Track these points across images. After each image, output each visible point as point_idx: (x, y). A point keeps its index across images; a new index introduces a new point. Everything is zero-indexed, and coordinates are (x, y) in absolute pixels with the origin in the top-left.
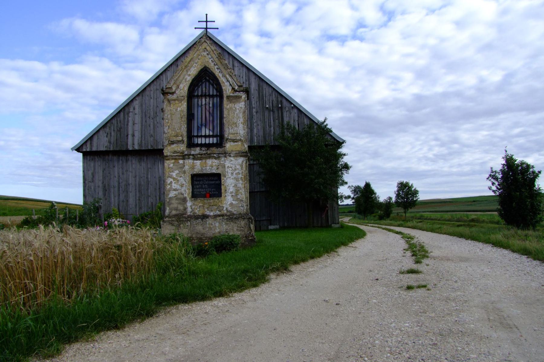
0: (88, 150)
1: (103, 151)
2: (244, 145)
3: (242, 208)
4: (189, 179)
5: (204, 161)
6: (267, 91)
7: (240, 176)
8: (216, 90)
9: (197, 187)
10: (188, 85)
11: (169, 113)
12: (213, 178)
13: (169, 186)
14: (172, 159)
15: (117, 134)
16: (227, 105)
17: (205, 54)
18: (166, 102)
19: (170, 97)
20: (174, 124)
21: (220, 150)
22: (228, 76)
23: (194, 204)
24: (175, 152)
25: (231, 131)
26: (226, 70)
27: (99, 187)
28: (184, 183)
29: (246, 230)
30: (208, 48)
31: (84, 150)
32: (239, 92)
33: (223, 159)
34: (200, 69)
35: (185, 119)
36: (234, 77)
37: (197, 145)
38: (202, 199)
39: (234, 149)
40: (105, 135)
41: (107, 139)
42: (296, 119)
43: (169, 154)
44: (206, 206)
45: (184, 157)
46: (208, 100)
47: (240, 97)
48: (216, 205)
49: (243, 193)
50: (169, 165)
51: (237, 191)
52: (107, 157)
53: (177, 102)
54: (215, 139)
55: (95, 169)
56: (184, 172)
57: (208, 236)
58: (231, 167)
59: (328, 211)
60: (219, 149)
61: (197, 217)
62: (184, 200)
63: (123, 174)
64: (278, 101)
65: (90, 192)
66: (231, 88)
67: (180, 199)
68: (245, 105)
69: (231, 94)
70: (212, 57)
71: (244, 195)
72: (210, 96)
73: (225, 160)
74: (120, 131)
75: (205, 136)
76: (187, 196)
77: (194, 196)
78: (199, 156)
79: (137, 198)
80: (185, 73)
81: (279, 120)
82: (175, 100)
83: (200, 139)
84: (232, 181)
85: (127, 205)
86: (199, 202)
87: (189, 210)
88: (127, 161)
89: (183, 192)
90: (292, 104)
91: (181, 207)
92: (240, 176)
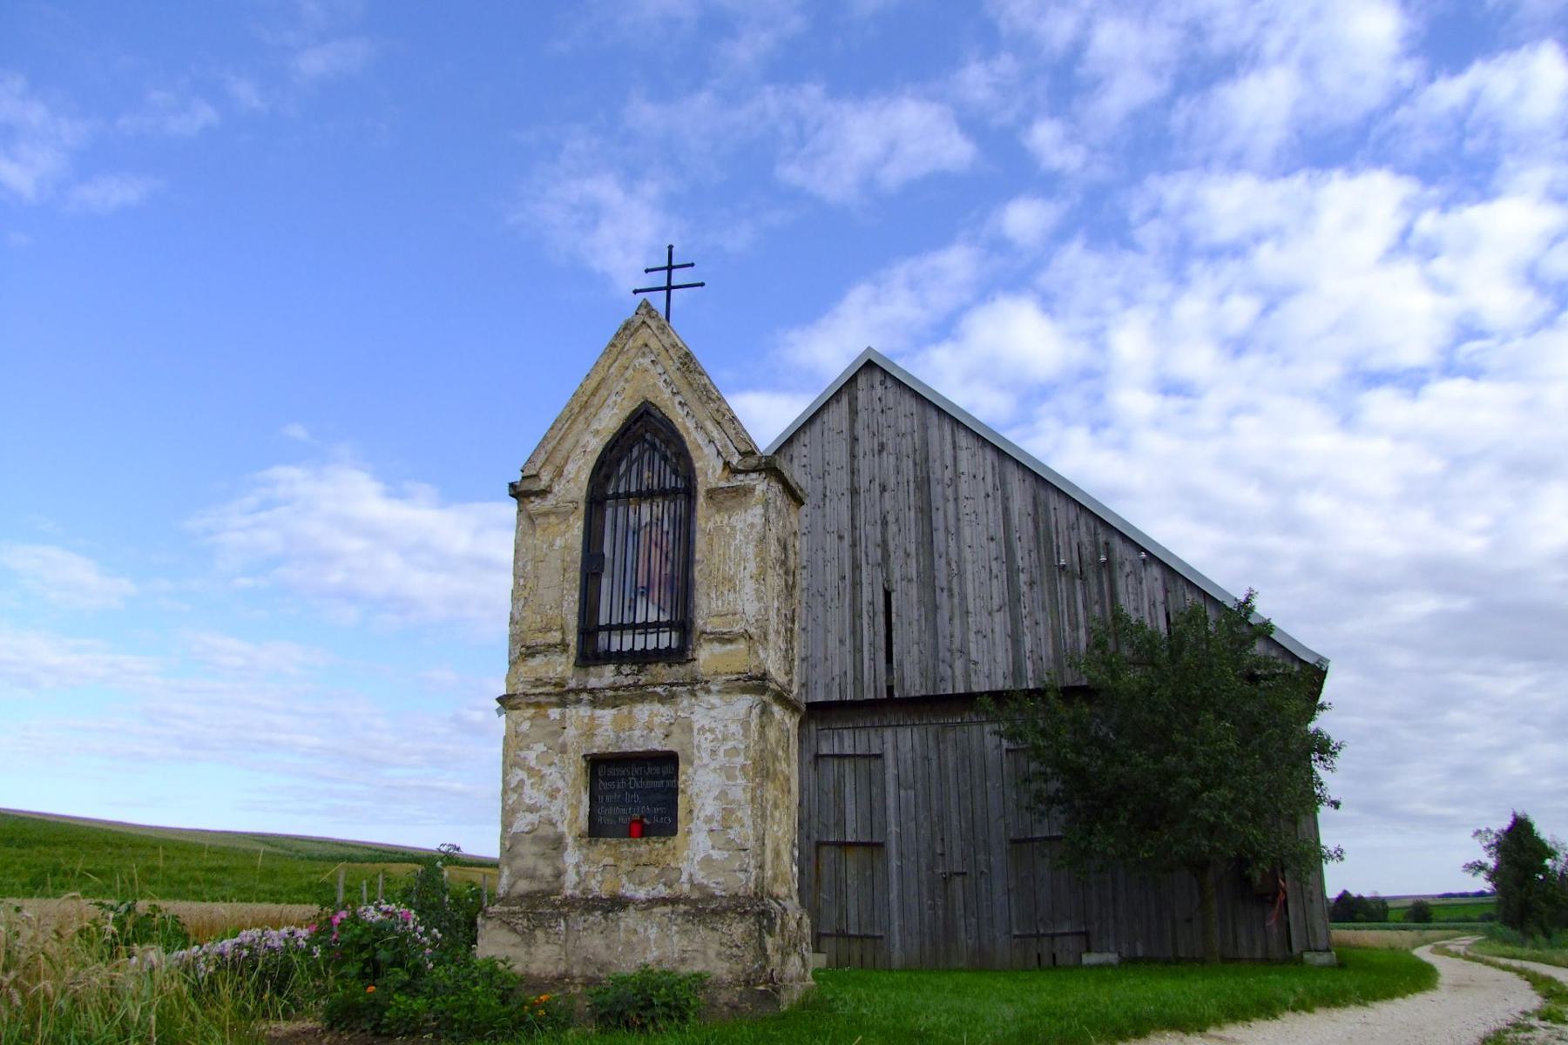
3: (742, 876)
4: (575, 768)
5: (625, 709)
6: (1061, 515)
8: (675, 472)
10: (592, 464)
13: (515, 797)
14: (529, 705)
17: (646, 362)
20: (540, 591)
21: (679, 671)
22: (709, 425)
24: (538, 682)
25: (717, 605)
26: (704, 404)
28: (560, 784)
29: (749, 957)
30: (654, 343)
32: (746, 472)
33: (685, 702)
34: (627, 413)
35: (575, 574)
36: (726, 425)
38: (614, 841)
39: (722, 669)
42: (1160, 597)
44: (625, 866)
45: (564, 696)
48: (655, 864)
49: (748, 822)
53: (553, 519)
56: (563, 750)
58: (712, 730)
59: (1285, 903)
60: (676, 668)
61: (590, 904)
62: (558, 844)
64: (1096, 544)
66: (719, 464)
69: (723, 484)
76: (566, 829)
77: (596, 830)
78: (610, 693)
80: (580, 424)
81: (1103, 607)
82: (546, 514)
84: (712, 776)
86: (603, 852)
87: (571, 878)
89: (556, 817)
91: (546, 870)
92: (740, 760)
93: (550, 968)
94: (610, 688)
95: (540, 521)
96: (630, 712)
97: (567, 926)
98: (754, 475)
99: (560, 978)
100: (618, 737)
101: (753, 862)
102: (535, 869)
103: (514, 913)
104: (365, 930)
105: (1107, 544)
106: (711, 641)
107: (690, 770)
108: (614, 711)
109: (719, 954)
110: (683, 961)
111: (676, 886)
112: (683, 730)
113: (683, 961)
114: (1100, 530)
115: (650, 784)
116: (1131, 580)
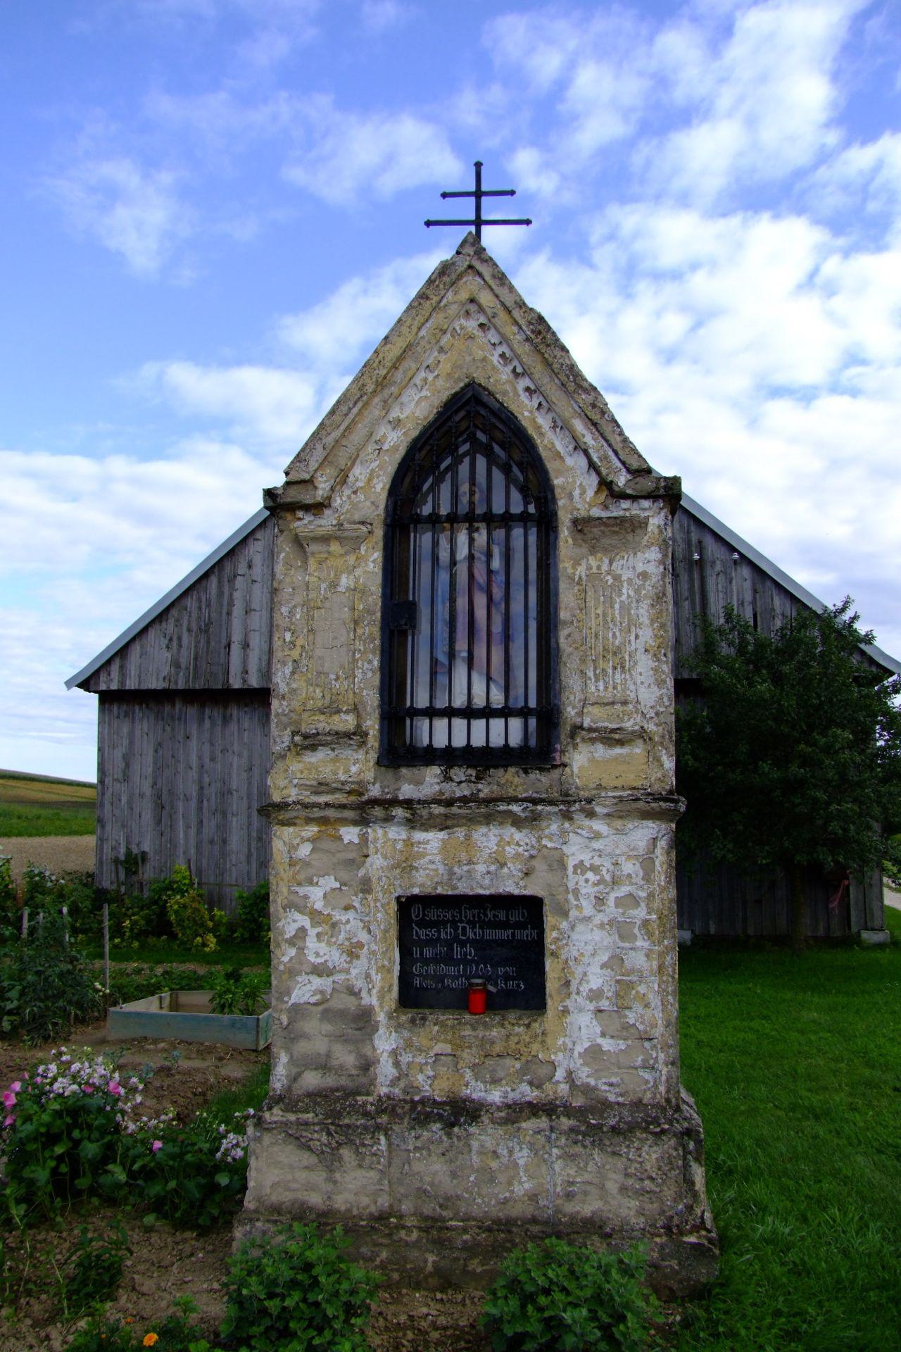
0: (114, 687)
1: (155, 691)
2: (658, 760)
3: (646, 1075)
4: (386, 917)
5: (460, 833)
7: (640, 913)
8: (524, 490)
9: (428, 952)
11: (298, 599)
12: (502, 915)
14: (309, 820)
15: (198, 643)
16: (577, 563)
17: (471, 325)
18: (285, 551)
19: (304, 524)
20: (318, 652)
21: (540, 781)
22: (579, 426)
23: (409, 1045)
24: (322, 786)
25: (596, 689)
27: (142, 796)
28: (363, 936)
29: (669, 1193)
30: (486, 299)
31: (103, 687)
32: (634, 498)
33: (554, 827)
34: (445, 396)
35: (372, 629)
37: (430, 756)
38: (448, 1018)
39: (608, 781)
40: (165, 642)
41: (168, 655)
42: (748, 596)
43: (293, 794)
44: (468, 1056)
45: (366, 809)
46: (481, 538)
47: (638, 525)
48: (516, 1055)
49: (655, 1000)
50: (292, 848)
51: (624, 989)
52: (167, 708)
53: (335, 547)
54: (516, 724)
55: (131, 743)
56: (366, 887)
57: (476, 1211)
58: (595, 869)
61: (422, 1112)
62: (363, 1021)
63: (213, 759)
64: (689, 543)
65: (117, 812)
66: (593, 480)
67: (342, 1014)
68: (662, 562)
69: (596, 512)
70: (504, 340)
71: (655, 1006)
72: (490, 519)
73: (564, 833)
74: (207, 631)
75: (469, 713)
76: (374, 1001)
77: (413, 997)
78: (438, 810)
79: (254, 834)
80: (375, 411)
81: (693, 603)
82: (325, 539)
83: (441, 724)
84: (598, 935)
85: (224, 854)
87: (385, 1070)
88: (226, 720)
89: (359, 984)
90: (733, 549)
91: (346, 1057)
92: (640, 913)
93: (365, 1201)
94: (438, 802)
95: (313, 548)
96: (468, 837)
97: (390, 1145)
98: (646, 504)
99: (382, 1217)
100: (451, 873)
101: (662, 1056)
102: (328, 1055)
103: (307, 1124)
104: (58, 1114)
105: (700, 542)
106: (593, 741)
107: (564, 925)
108: (442, 835)
109: (623, 1189)
110: (569, 1196)
111: (547, 1086)
112: (551, 868)
113: (569, 1196)
114: (693, 528)
115: (490, 934)
116: (722, 577)
